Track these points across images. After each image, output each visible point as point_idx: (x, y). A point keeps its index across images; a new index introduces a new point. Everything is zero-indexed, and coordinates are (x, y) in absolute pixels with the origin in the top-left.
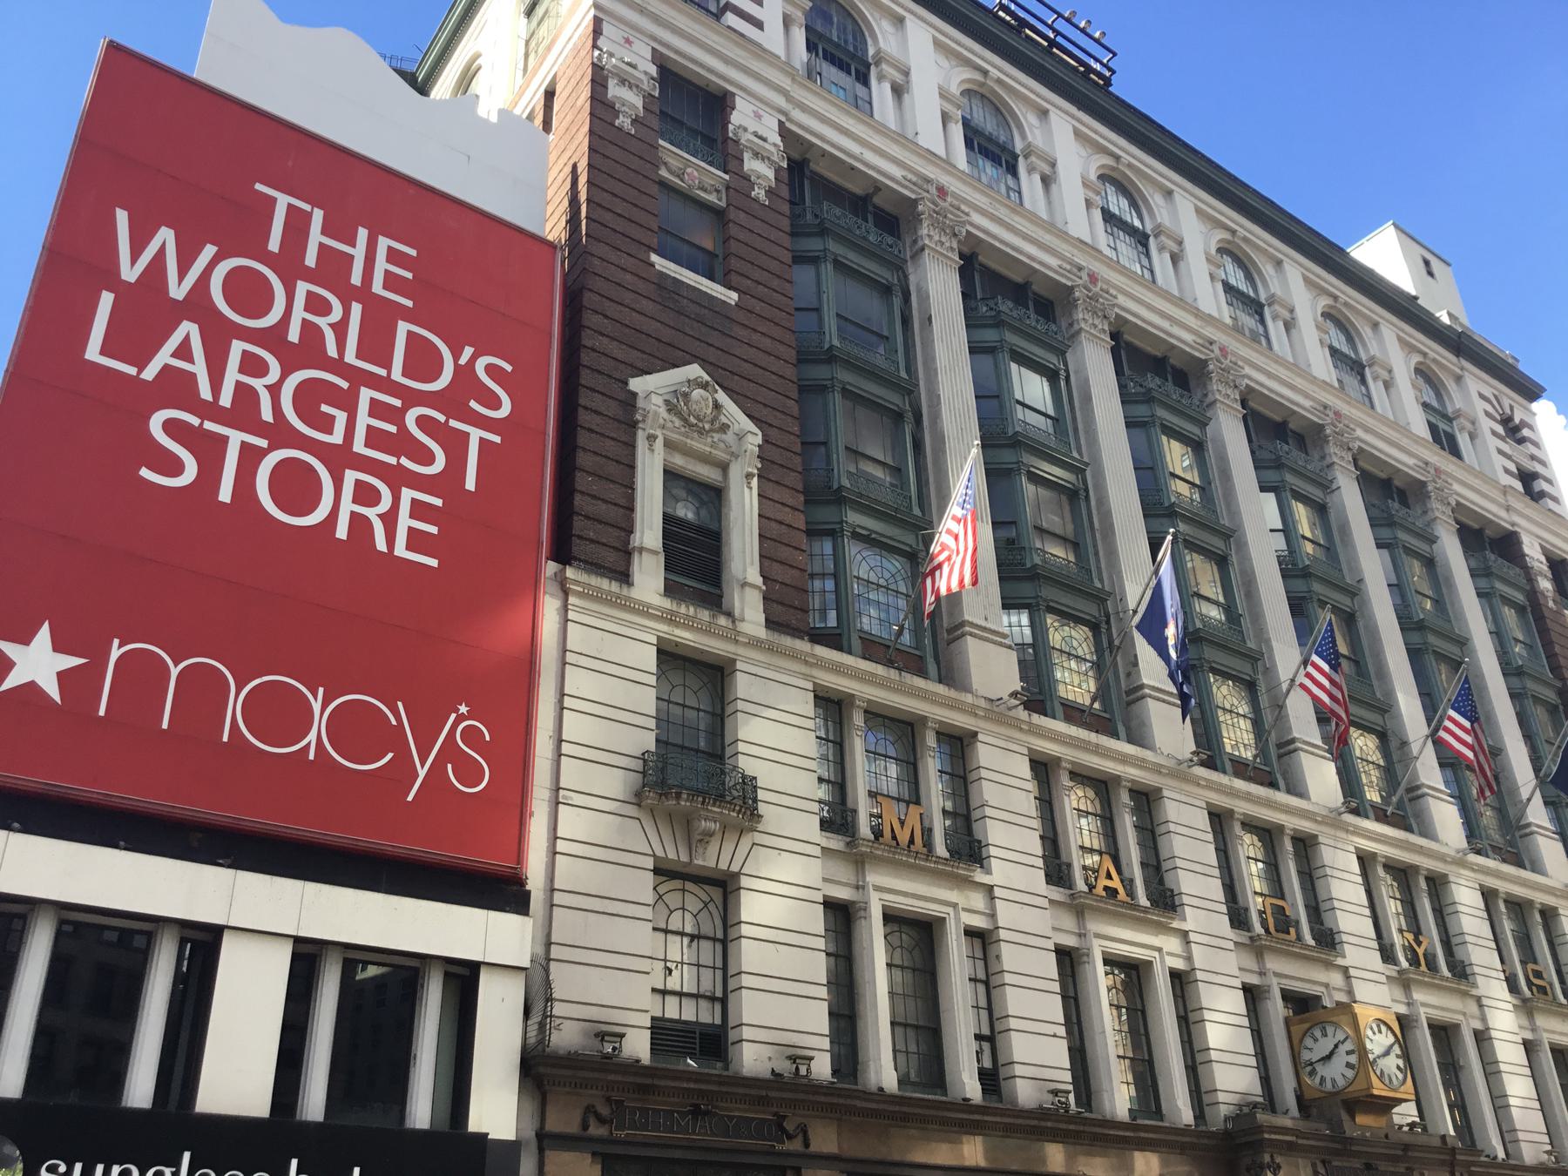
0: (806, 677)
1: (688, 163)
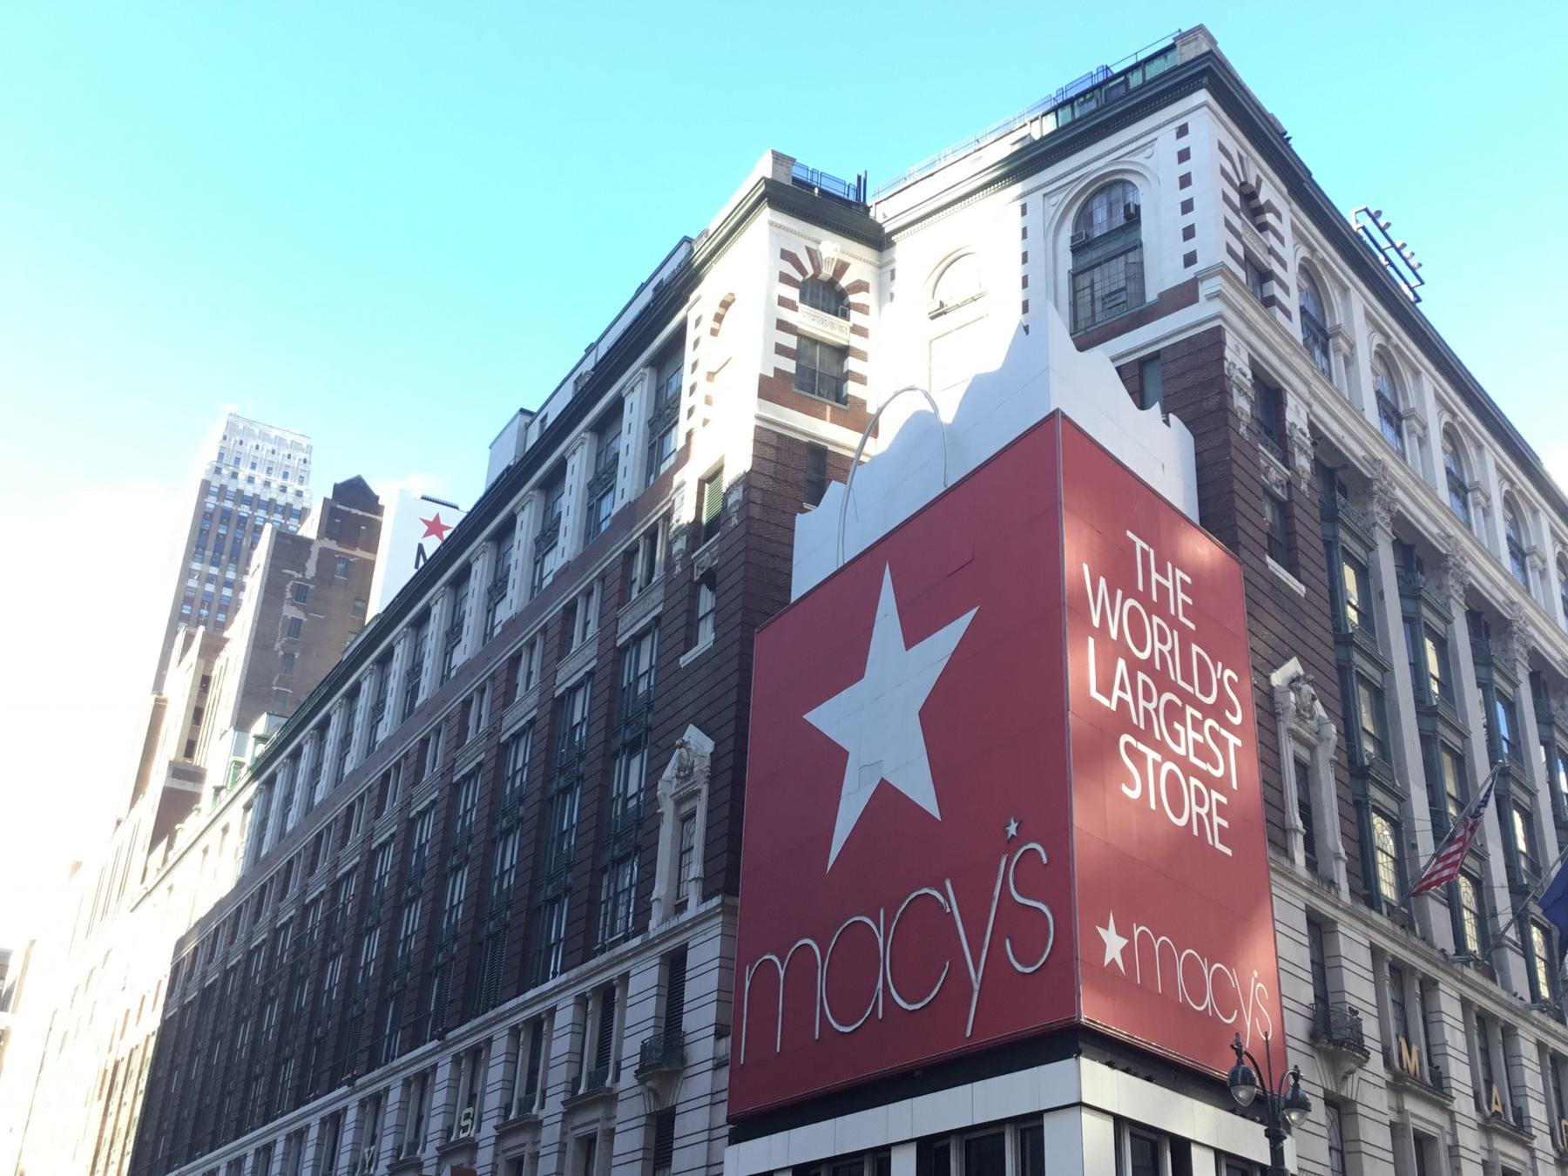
0: (1367, 936)
1: (1271, 464)
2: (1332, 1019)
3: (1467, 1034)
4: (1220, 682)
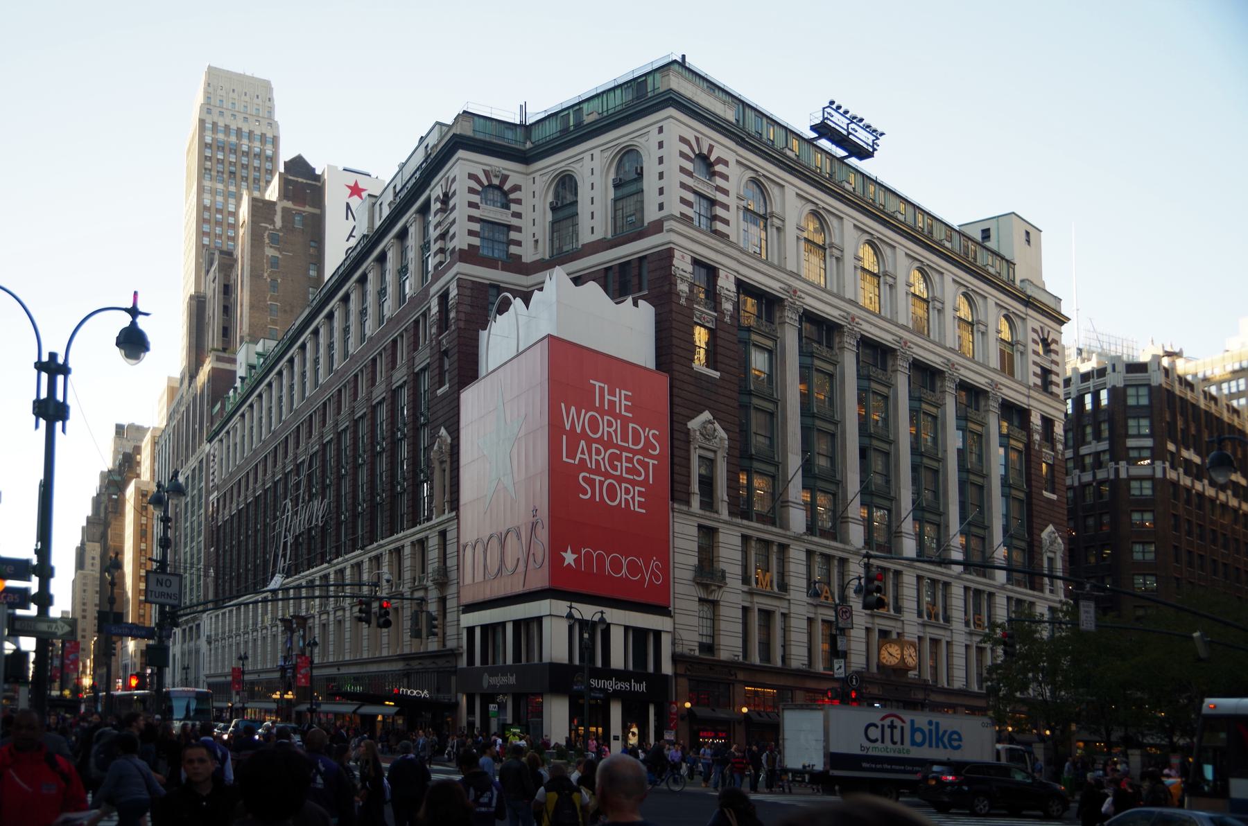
4: (647, 438)
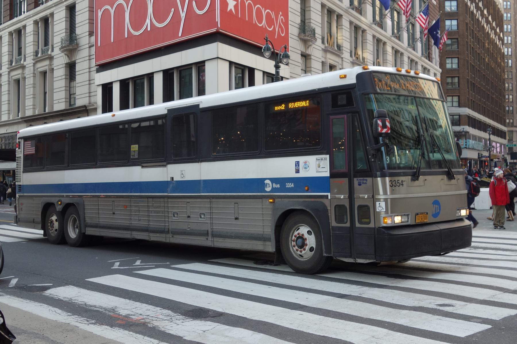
2: (306, 28)
3: (350, 32)
